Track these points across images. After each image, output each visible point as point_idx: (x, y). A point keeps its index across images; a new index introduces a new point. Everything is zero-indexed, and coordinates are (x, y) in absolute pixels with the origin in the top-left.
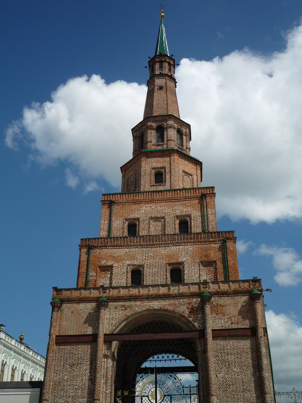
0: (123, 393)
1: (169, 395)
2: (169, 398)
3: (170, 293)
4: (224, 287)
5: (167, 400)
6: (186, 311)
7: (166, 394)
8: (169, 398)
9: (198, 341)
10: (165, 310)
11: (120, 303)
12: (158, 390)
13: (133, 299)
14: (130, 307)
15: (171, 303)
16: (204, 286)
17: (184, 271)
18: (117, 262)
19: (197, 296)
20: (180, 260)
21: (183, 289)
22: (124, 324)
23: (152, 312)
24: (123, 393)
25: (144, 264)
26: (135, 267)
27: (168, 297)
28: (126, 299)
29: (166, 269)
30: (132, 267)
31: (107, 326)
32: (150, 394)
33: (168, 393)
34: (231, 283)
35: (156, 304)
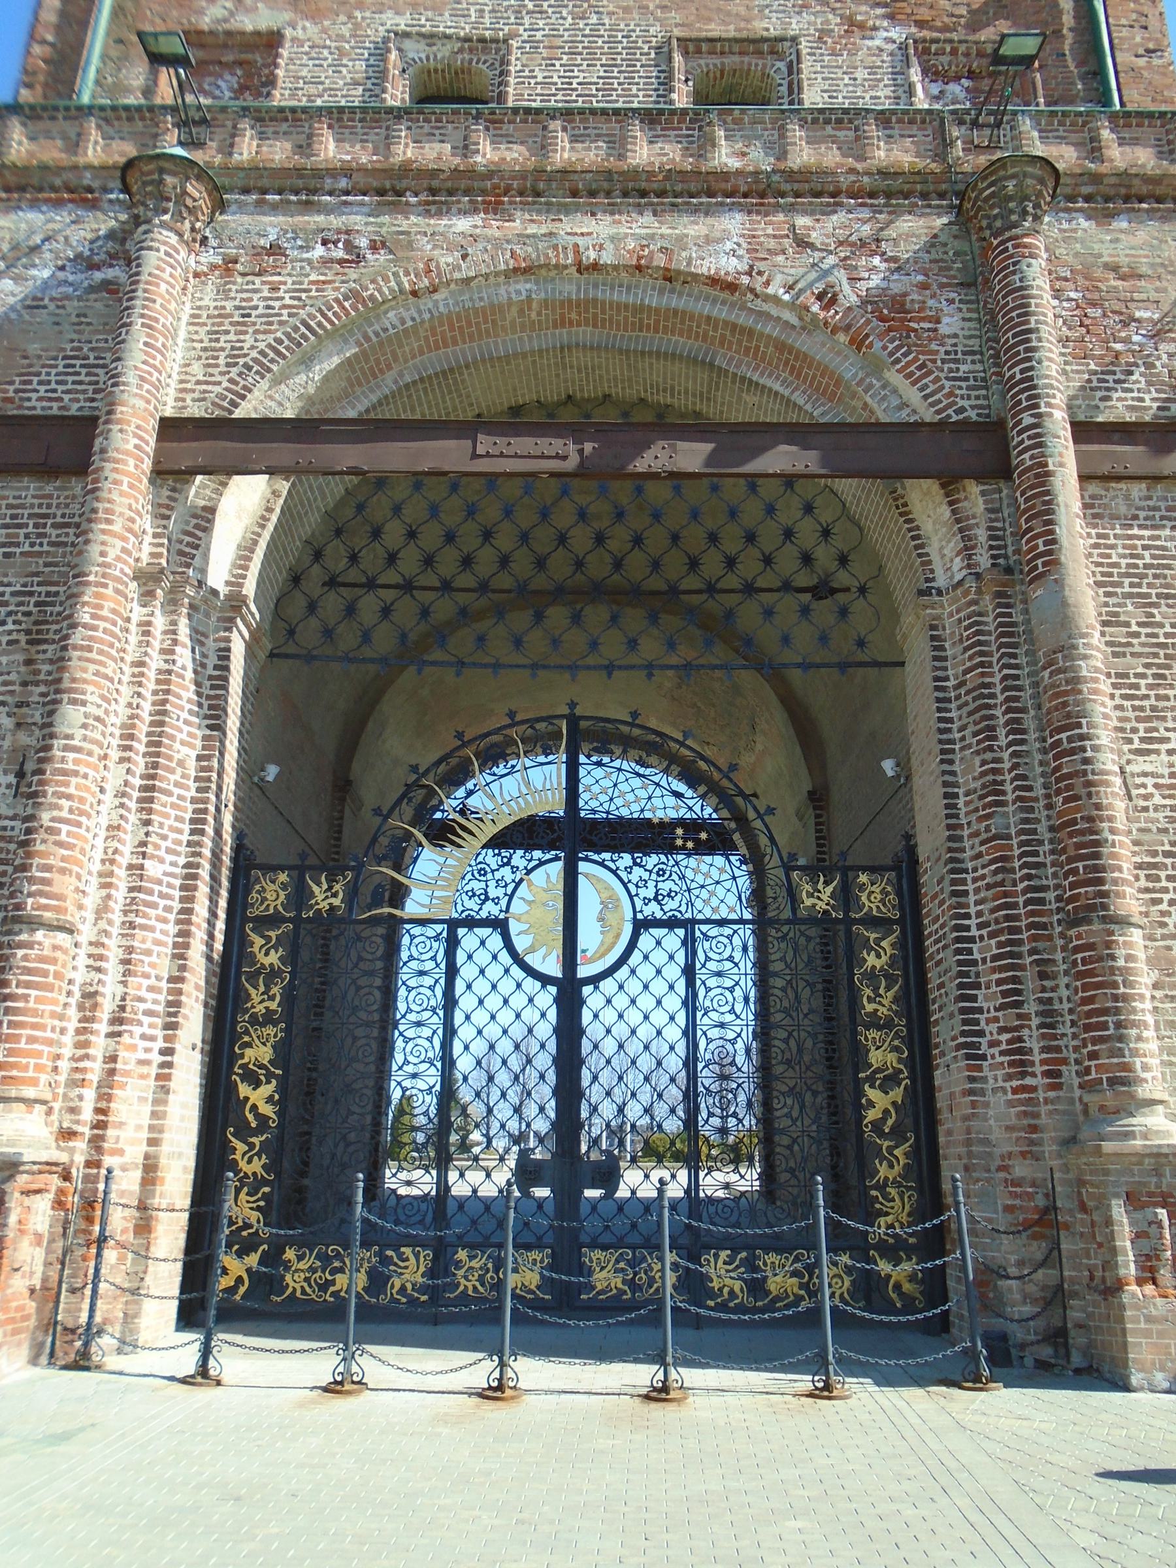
0: (299, 896)
1: (671, 923)
2: (673, 940)
5: (659, 957)
8: (673, 940)
17: (795, 89)
19: (924, 196)
20: (769, 26)
22: (336, 360)
23: (570, 288)
24: (299, 896)
26: (443, 51)
30: (416, 50)
31: (197, 369)
32: (517, 906)
33: (670, 905)
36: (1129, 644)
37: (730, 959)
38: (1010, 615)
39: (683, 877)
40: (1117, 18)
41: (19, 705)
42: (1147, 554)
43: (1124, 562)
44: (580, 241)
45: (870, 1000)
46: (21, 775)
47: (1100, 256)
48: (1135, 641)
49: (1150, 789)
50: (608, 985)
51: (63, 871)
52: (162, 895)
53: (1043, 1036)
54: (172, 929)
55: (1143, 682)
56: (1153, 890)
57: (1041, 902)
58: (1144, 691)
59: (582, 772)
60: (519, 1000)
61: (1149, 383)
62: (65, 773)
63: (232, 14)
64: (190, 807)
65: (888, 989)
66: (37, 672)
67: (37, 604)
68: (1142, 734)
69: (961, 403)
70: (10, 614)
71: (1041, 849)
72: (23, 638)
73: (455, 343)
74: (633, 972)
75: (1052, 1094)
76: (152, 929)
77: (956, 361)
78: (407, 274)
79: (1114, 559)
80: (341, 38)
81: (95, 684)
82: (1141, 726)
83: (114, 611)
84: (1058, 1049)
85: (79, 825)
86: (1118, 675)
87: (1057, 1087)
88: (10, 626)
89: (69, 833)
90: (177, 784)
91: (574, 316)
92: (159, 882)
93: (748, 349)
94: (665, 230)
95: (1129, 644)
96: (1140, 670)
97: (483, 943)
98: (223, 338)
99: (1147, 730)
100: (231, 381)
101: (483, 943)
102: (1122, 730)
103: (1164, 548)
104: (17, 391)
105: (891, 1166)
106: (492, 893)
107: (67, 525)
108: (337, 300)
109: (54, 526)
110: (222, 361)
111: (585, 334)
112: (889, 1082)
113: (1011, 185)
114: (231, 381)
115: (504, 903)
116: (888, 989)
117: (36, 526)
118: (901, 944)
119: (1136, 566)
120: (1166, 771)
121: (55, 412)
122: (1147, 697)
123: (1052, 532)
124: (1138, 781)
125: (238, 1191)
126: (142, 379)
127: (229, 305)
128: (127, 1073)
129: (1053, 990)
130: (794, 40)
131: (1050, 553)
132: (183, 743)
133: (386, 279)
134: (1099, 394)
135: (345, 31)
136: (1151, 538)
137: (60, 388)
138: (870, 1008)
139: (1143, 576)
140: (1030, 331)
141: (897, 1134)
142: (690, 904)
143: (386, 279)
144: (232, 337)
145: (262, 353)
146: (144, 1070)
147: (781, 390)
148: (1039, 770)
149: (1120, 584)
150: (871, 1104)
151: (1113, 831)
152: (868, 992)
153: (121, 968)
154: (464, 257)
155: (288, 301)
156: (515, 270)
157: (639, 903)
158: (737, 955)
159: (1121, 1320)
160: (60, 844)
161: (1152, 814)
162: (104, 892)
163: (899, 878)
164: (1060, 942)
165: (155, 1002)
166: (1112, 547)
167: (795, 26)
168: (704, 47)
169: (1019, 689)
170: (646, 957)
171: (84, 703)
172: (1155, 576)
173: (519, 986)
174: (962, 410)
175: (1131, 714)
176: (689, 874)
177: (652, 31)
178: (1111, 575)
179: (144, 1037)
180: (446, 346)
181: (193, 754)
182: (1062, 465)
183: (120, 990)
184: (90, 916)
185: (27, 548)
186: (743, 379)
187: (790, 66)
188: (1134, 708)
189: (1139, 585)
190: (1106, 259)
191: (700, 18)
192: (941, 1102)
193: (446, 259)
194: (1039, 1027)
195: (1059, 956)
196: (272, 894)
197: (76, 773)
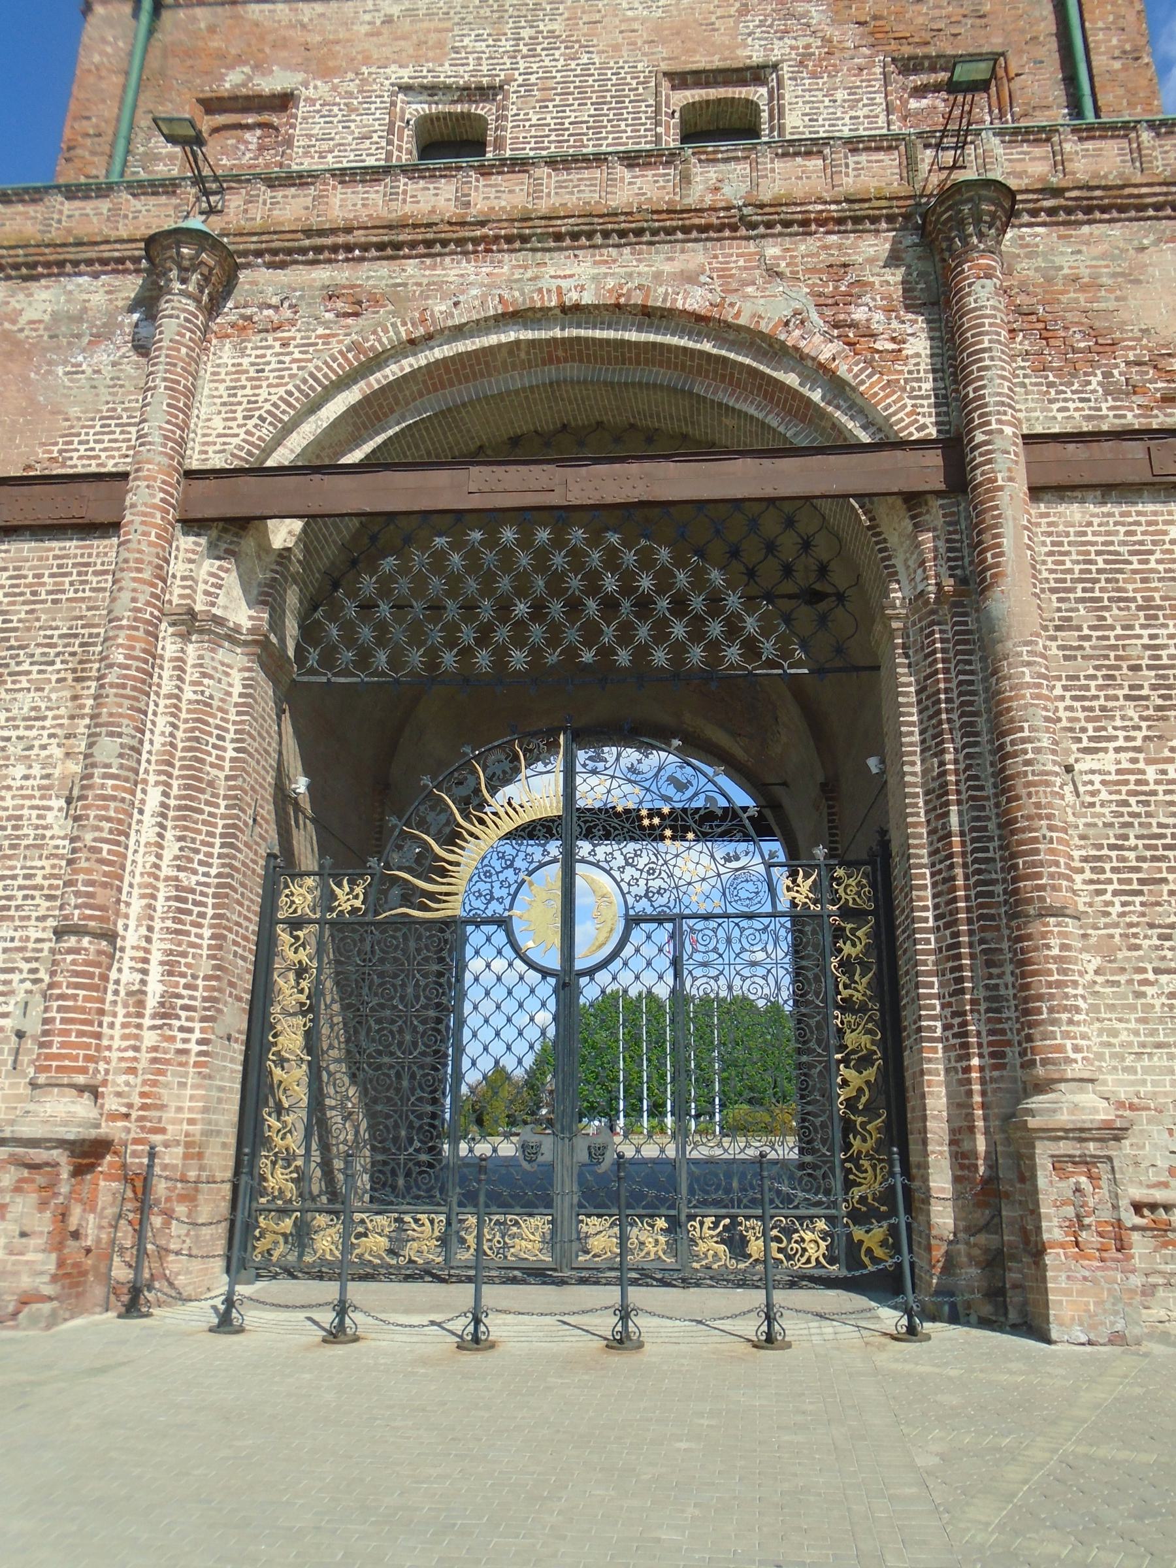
1: (659, 920)
2: (662, 934)
3: (691, 201)
4: (1098, 161)
5: (649, 950)
6: (814, 316)
7: (644, 906)
8: (662, 934)
9: (896, 527)
10: (649, 316)
11: (322, 275)
12: (579, 882)
13: (413, 245)
14: (395, 297)
15: (692, 266)
16: (948, 157)
17: (777, 112)
18: (326, 73)
21: (782, 179)
25: (508, 81)
27: (670, 231)
28: (365, 248)
29: (658, 105)
31: (218, 423)
34: (1146, 136)
35: (580, 277)
36: (1081, 648)
37: (715, 950)
38: (965, 623)
39: (671, 876)
40: (1094, 22)
41: (68, 736)
42: (1100, 559)
43: (1077, 568)
44: (564, 284)
45: (846, 987)
46: (69, 801)
47: (1061, 268)
48: (1086, 644)
49: (1097, 786)
50: (603, 977)
51: (105, 885)
52: (196, 903)
53: (989, 1020)
54: (207, 933)
55: (1093, 684)
56: (1098, 882)
57: (990, 894)
58: (1093, 692)
59: (579, 780)
60: (521, 992)
61: (1107, 393)
62: (104, 798)
63: (250, 78)
64: (221, 823)
65: (863, 976)
66: (82, 706)
67: (82, 645)
68: (1091, 733)
69: (922, 420)
70: (58, 654)
71: (991, 845)
72: (70, 676)
73: (452, 385)
74: (625, 964)
75: (996, 1074)
76: (187, 934)
77: (919, 380)
78: (404, 324)
79: (1068, 565)
80: (350, 94)
81: (130, 717)
82: (1090, 726)
83: (145, 651)
84: (1003, 1032)
85: (118, 843)
86: (1069, 678)
87: (1002, 1067)
88: (58, 666)
89: (109, 852)
90: (208, 803)
91: (560, 353)
92: (193, 891)
93: (723, 376)
94: (642, 268)
95: (1081, 648)
96: (1091, 672)
97: (488, 939)
98: (240, 393)
99: (1096, 729)
100: (248, 433)
101: (488, 939)
102: (1071, 730)
103: (1117, 553)
104: (60, 452)
105: (864, 1140)
106: (497, 893)
107: (105, 572)
108: (341, 352)
109: (96, 573)
110: (239, 415)
111: (572, 370)
112: (864, 1062)
113: (966, 208)
114: (248, 433)
115: (507, 902)
116: (863, 976)
117: (79, 574)
118: (875, 934)
119: (1089, 571)
120: (1113, 768)
121: (94, 469)
122: (1097, 697)
123: (999, 545)
124: (1086, 778)
125: (274, 1163)
126: (166, 437)
127: (245, 361)
128: (167, 1062)
129: (1000, 976)
130: (775, 67)
131: (998, 565)
132: (212, 765)
133: (386, 331)
134: (1055, 406)
135: (353, 87)
136: (1104, 544)
137: (98, 446)
138: (846, 993)
139: (1098, 581)
140: (984, 350)
141: (870, 1111)
142: (678, 900)
143: (386, 331)
144: (248, 391)
145: (275, 405)
146: (183, 1059)
147: (755, 414)
148: (990, 770)
149: (1072, 590)
150: (845, 1083)
151: (1051, 828)
152: (844, 979)
153: (160, 969)
154: (456, 304)
155: (297, 356)
156: (503, 315)
157: (630, 900)
158: (722, 947)
159: (1044, 1279)
160: (102, 861)
161: (1098, 809)
162: (144, 902)
163: (874, 871)
164: (1006, 932)
165: (192, 998)
166: (1067, 553)
167: (779, 50)
168: (690, 79)
169: (973, 693)
170: (637, 950)
171: (120, 735)
172: (1108, 581)
173: (521, 978)
174: (923, 427)
175: (1081, 715)
176: (677, 872)
177: (640, 66)
178: (1064, 581)
179: (182, 1029)
180: (443, 387)
181: (222, 775)
182: (1011, 479)
183: (160, 988)
184: (132, 923)
185: (71, 595)
186: (720, 404)
187: (771, 93)
188: (1084, 709)
189: (1092, 590)
190: (1066, 271)
191: (687, 51)
192: (908, 1083)
193: (440, 307)
194: (988, 1011)
195: (1005, 945)
196: (301, 897)
197: (114, 798)
